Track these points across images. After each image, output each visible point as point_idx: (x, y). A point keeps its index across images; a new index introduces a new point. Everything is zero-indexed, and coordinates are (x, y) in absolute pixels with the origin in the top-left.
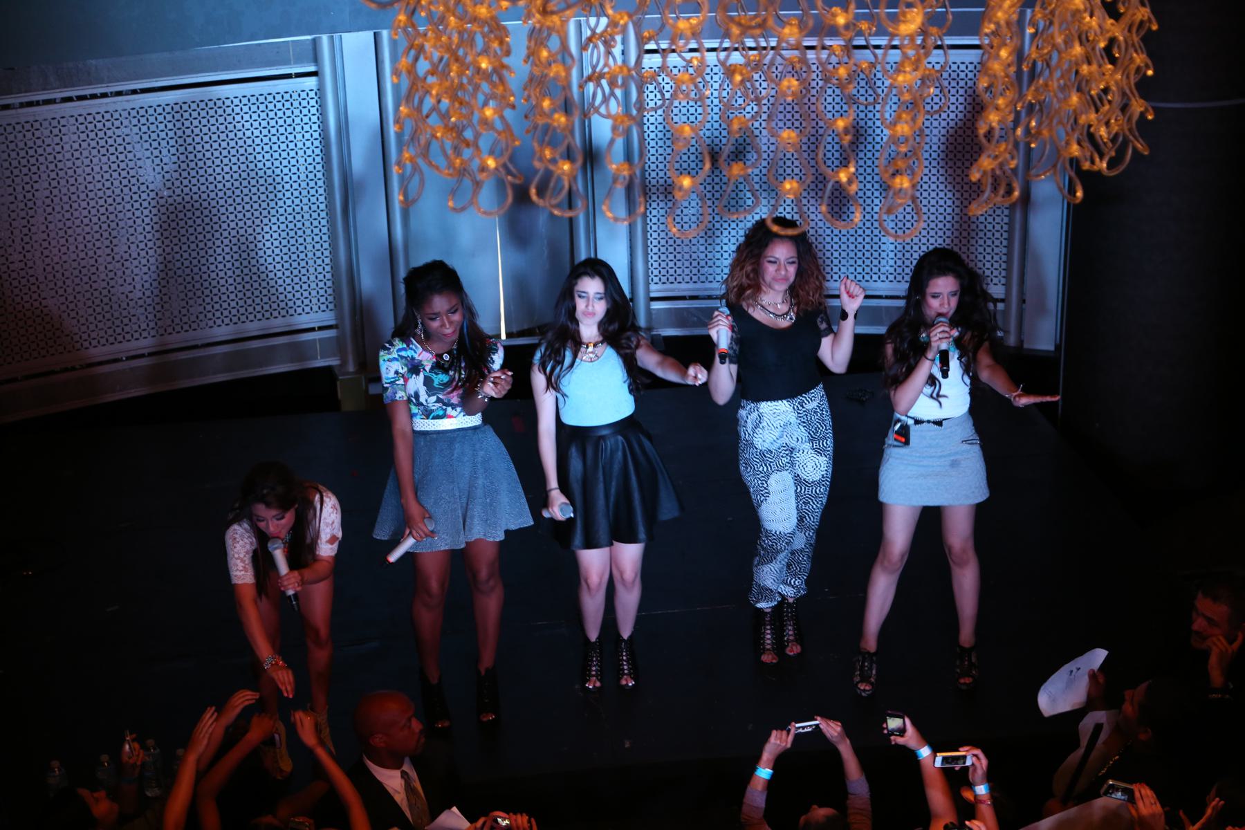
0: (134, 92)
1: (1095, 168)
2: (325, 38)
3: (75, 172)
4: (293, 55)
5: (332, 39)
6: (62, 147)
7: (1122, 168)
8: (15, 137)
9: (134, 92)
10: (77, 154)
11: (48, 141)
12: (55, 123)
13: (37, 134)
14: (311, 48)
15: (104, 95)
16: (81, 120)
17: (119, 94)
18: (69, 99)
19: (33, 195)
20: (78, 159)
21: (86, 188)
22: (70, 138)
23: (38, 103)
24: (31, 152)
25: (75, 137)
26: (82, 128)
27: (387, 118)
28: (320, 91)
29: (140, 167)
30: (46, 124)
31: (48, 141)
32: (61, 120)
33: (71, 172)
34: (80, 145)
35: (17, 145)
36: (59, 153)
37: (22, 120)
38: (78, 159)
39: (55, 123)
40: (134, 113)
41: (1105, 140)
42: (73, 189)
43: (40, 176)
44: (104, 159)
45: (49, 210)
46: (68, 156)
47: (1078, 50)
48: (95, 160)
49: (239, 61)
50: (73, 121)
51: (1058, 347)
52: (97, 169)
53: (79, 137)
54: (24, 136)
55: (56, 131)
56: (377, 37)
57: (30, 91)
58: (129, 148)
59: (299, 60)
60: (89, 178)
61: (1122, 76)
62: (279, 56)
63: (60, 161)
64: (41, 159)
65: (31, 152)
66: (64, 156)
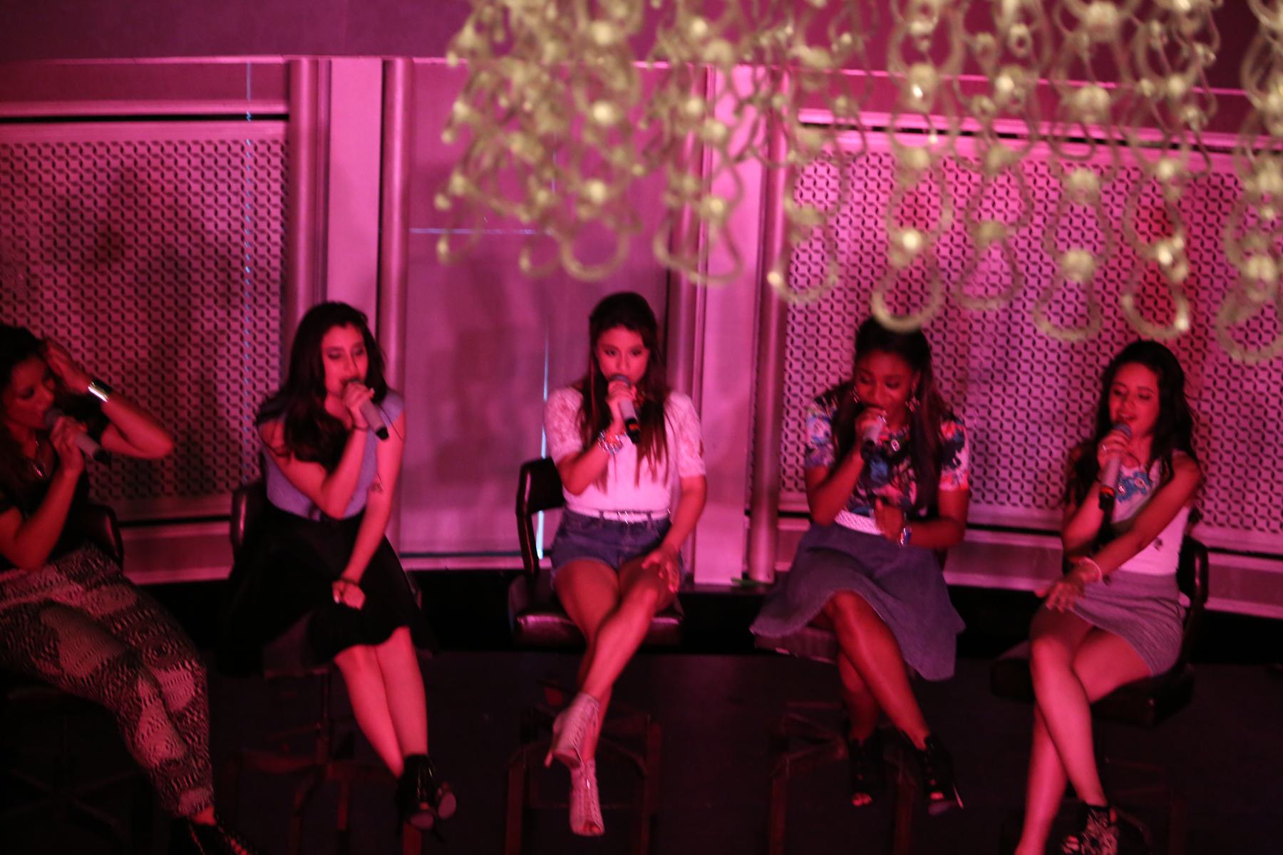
2: (305, 62)
4: (252, 86)
5: (315, 66)
27: (391, 193)
28: (289, 145)
56: (387, 69)
59: (259, 95)
62: (228, 83)
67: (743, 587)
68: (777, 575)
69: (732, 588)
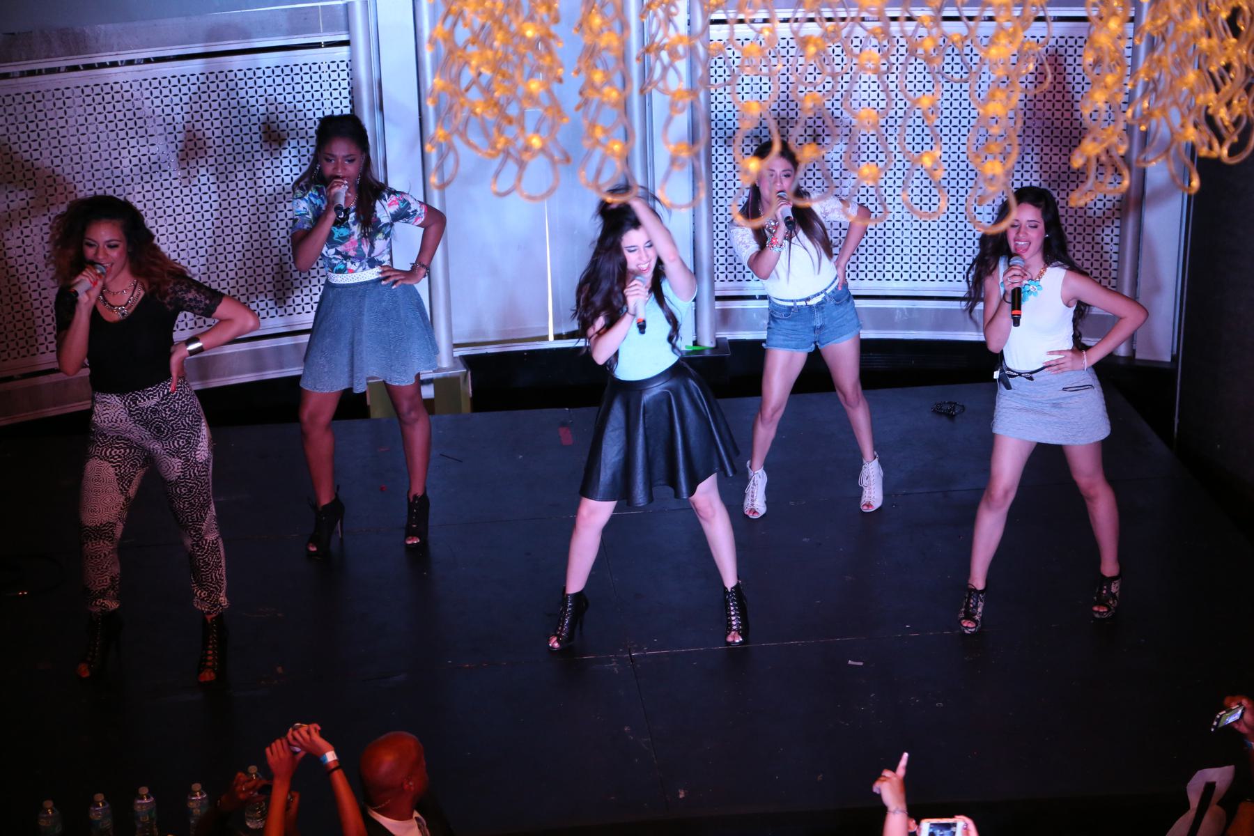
0: (147, 61)
1: (1214, 154)
3: (80, 149)
6: (67, 121)
7: (1244, 155)
8: (15, 110)
9: (147, 61)
10: (82, 129)
11: (50, 115)
12: (58, 94)
13: (39, 106)
14: (342, 13)
15: (114, 64)
16: (87, 91)
17: (130, 63)
18: (75, 68)
19: (34, 174)
20: (83, 134)
21: (92, 166)
22: (75, 111)
23: (40, 72)
24: (32, 126)
25: (80, 111)
26: (88, 100)
29: (153, 145)
30: (48, 96)
31: (50, 115)
32: (66, 91)
33: (75, 149)
34: (86, 120)
35: (16, 118)
36: (62, 127)
37: (23, 90)
38: (83, 134)
39: (58, 94)
40: (146, 84)
41: (1227, 123)
42: (77, 168)
43: (41, 153)
44: (113, 135)
45: (51, 191)
46: (73, 131)
47: (1196, 21)
48: (103, 136)
49: (263, 28)
50: (78, 92)
51: (1174, 358)
52: (104, 146)
53: (85, 111)
54: (25, 108)
55: (59, 104)
57: (32, 59)
58: (140, 123)
59: (330, 28)
60: (96, 156)
61: (1247, 51)
63: (64, 137)
64: (43, 134)
65: (32, 126)
66: (68, 131)
67: (694, 351)
68: (717, 341)
69: (688, 352)
